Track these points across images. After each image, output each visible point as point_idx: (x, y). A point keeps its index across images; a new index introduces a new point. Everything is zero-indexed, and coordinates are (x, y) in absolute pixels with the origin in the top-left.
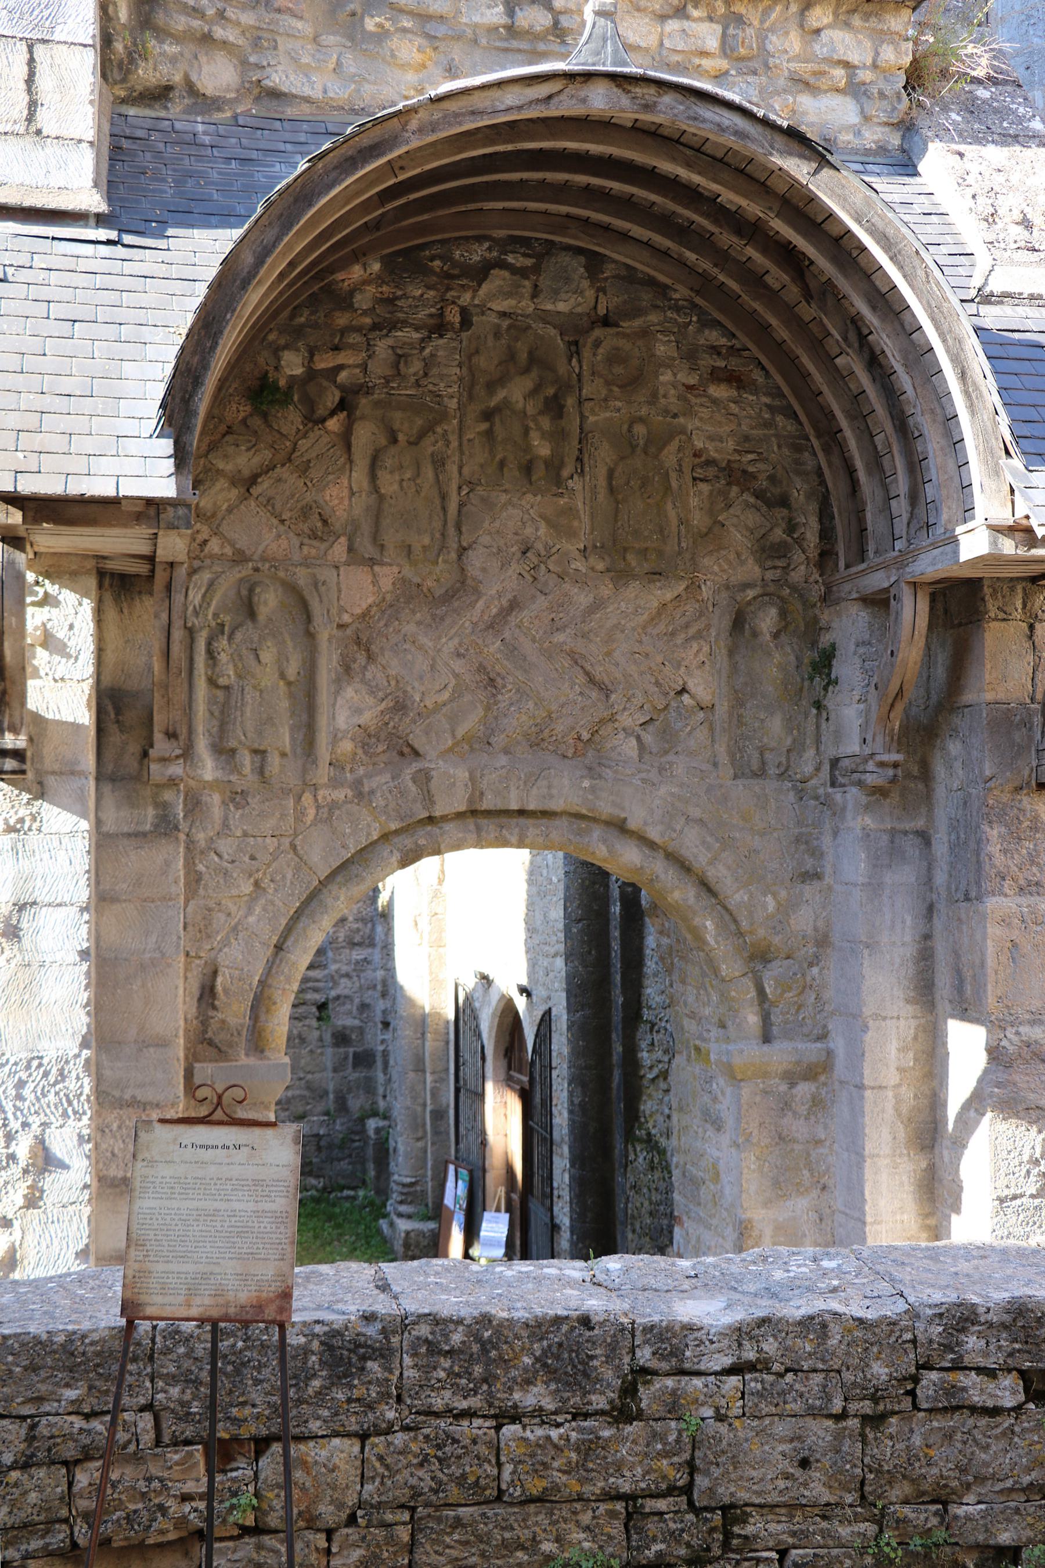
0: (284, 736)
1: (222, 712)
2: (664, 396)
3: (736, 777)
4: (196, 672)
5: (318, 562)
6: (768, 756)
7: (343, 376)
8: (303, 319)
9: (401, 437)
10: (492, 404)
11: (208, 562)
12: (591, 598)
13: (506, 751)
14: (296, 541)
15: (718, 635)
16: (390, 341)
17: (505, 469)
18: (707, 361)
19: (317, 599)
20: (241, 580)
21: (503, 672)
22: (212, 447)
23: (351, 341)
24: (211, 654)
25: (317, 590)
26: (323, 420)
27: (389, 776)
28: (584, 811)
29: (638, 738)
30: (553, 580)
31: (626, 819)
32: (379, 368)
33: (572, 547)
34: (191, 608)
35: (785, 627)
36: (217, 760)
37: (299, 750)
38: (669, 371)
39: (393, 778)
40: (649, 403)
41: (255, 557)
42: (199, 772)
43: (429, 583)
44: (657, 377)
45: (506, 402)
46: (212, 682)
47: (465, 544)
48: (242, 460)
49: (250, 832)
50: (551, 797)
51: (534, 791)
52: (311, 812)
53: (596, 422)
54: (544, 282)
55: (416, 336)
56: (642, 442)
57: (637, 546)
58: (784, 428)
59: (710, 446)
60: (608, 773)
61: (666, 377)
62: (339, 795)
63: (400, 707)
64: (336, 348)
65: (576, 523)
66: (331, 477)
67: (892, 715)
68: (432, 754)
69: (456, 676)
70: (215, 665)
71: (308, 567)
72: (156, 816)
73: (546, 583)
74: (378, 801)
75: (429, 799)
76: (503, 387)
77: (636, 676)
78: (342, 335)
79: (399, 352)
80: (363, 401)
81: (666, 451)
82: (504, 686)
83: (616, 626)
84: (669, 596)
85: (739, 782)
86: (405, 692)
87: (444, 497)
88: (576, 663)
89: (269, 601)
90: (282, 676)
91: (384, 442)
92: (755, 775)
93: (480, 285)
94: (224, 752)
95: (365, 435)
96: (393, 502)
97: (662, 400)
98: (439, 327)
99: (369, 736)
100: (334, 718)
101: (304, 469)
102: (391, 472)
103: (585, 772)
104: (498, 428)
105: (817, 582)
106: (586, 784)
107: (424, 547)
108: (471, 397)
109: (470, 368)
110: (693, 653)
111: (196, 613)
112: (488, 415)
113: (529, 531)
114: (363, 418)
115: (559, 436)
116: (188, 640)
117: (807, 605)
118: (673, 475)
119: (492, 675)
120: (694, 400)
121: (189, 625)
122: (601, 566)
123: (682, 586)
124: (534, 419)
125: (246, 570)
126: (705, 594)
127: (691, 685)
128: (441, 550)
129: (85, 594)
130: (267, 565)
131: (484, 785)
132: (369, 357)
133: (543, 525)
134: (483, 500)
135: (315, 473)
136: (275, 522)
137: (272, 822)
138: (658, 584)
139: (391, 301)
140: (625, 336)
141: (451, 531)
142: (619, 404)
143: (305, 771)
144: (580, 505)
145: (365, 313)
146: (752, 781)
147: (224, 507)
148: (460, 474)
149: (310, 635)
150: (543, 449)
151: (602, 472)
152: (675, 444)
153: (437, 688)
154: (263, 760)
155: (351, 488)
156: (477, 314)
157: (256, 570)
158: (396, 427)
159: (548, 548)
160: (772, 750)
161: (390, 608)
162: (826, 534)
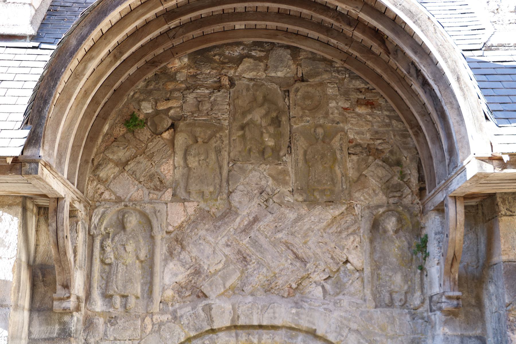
0: (138, 288)
1: (107, 277)
2: (332, 114)
3: (376, 307)
4: (94, 257)
5: (157, 201)
6: (395, 296)
7: (172, 112)
8: (152, 87)
9: (199, 140)
10: (245, 122)
11: (103, 203)
12: (296, 215)
13: (252, 294)
14: (146, 192)
15: (364, 232)
16: (194, 95)
17: (251, 153)
18: (355, 96)
19: (156, 219)
20: (119, 211)
21: (250, 254)
22: (107, 148)
23: (175, 95)
24: (102, 248)
25: (156, 215)
27: (190, 308)
28: (293, 326)
29: (323, 287)
30: (276, 206)
31: (315, 330)
32: (188, 108)
33: (285, 190)
34: (93, 225)
35: (402, 227)
36: (104, 301)
37: (145, 295)
38: (334, 102)
39: (192, 309)
40: (324, 117)
41: (126, 200)
42: (93, 307)
43: (213, 210)
44: (328, 105)
45: (252, 121)
46: (103, 262)
47: (231, 190)
48: (122, 154)
49: (118, 338)
50: (275, 318)
51: (266, 315)
52: (150, 327)
53: (297, 128)
54: (271, 62)
55: (207, 91)
56: (321, 137)
57: (320, 188)
58: (397, 126)
59: (357, 137)
60: (306, 305)
61: (333, 104)
62: (165, 318)
63: (197, 272)
64: (168, 99)
65: (287, 178)
66: (164, 160)
67: (453, 270)
68: (212, 295)
69: (226, 256)
70: (104, 253)
71: (151, 203)
72: (60, 329)
73: (273, 208)
74: (184, 321)
75: (211, 320)
76: (250, 113)
77: (320, 254)
78: (171, 93)
79: (199, 99)
80: (181, 124)
81: (334, 140)
82: (251, 261)
83: (309, 229)
84: (337, 213)
85: (378, 310)
86: (200, 265)
87: (221, 167)
88: (289, 248)
89: (133, 221)
90: (138, 258)
91: (191, 142)
92: (388, 306)
93: (238, 67)
94: (107, 297)
95: (181, 139)
97: (331, 116)
98: (219, 87)
99: (182, 287)
100: (163, 278)
101: (150, 157)
102: (194, 157)
103: (293, 305)
104: (248, 135)
105: (418, 204)
106: (294, 311)
107: (211, 192)
108: (234, 120)
109: (234, 106)
110: (350, 242)
111: (95, 228)
112: (243, 128)
113: (263, 183)
114: (181, 131)
115: (277, 136)
116: (91, 241)
117: (413, 215)
118: (338, 152)
119: (245, 255)
120: (347, 115)
121: (92, 233)
122: (300, 199)
123: (343, 208)
124: (266, 128)
125: (121, 206)
126: (356, 211)
127: (350, 259)
128: (219, 194)
129: (16, 215)
130: (131, 203)
131: (239, 312)
132: (184, 103)
133: (270, 179)
134: (240, 168)
135: (156, 159)
136: (137, 183)
137: (129, 333)
138: (331, 207)
139: (194, 76)
140: (311, 86)
141: (225, 184)
142: (308, 119)
143: (147, 306)
144: (290, 169)
145: (182, 82)
146: (386, 309)
147: (112, 176)
148: (229, 156)
149: (152, 237)
150: (270, 143)
151: (301, 152)
152: (338, 136)
153: (216, 262)
154: (127, 300)
155: (174, 165)
156: (237, 80)
157: (126, 206)
158: (198, 134)
159: (273, 190)
160: (396, 292)
161: (193, 223)
162: (421, 179)
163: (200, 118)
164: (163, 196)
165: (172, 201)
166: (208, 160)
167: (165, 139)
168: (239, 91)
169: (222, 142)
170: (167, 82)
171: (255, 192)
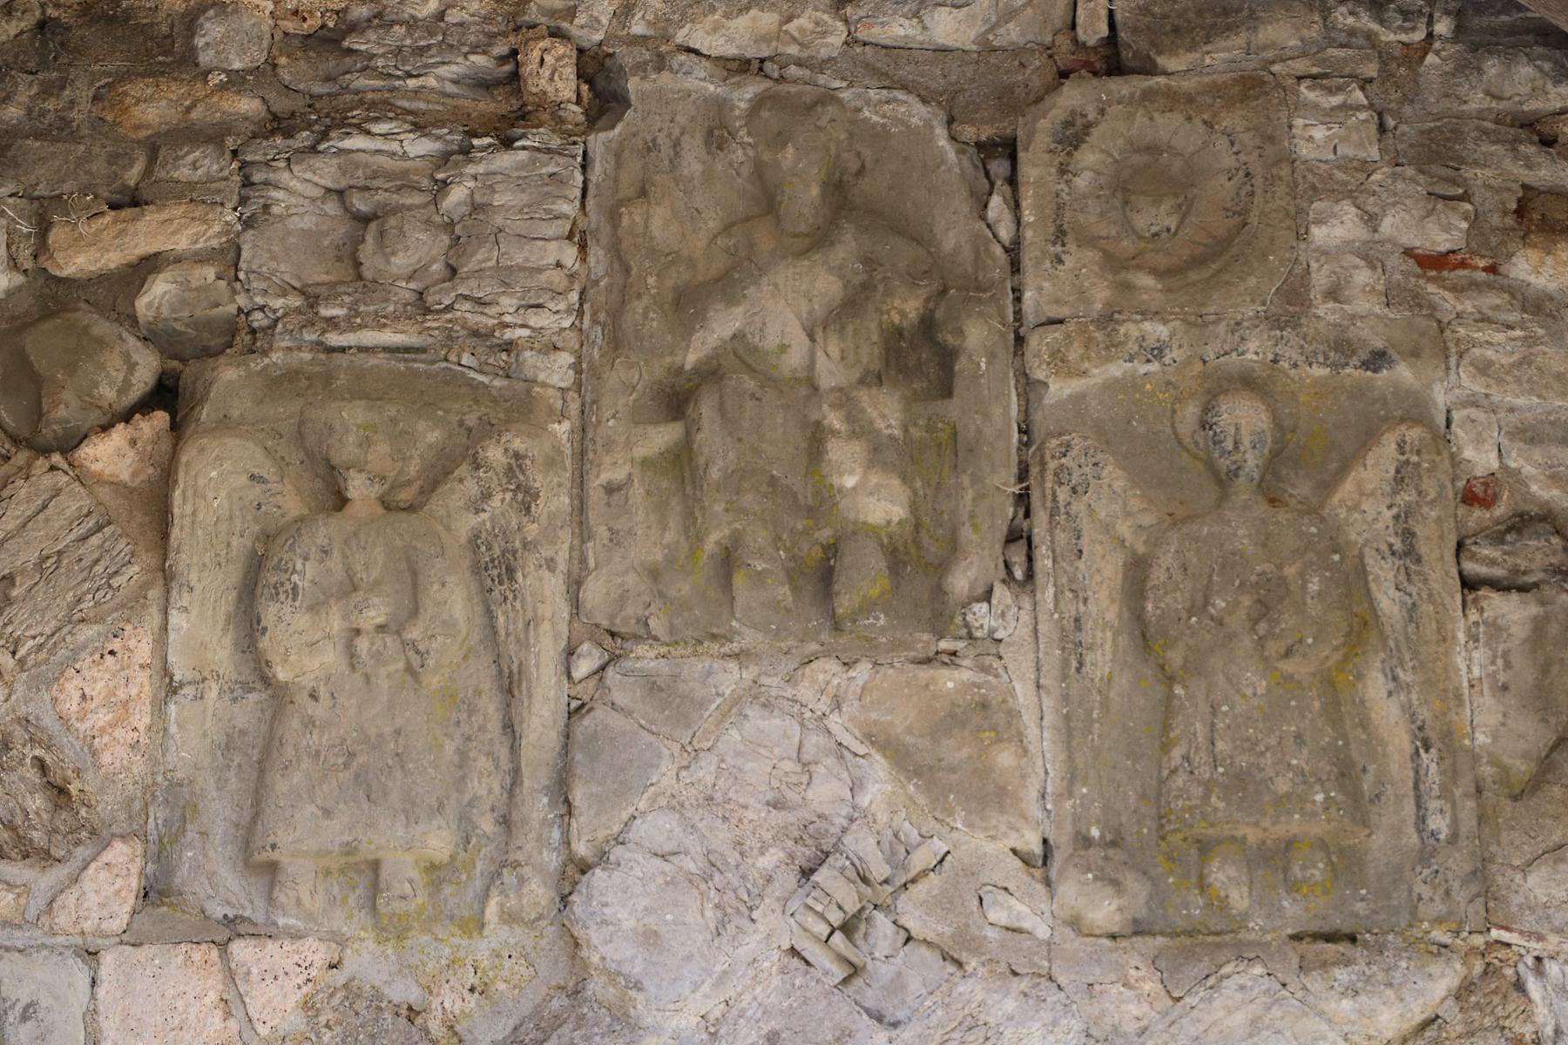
2: (1333, 294)
5: (19, 938)
7: (158, 294)
9: (358, 487)
10: (691, 359)
16: (324, 171)
17: (739, 580)
18: (1502, 170)
23: (183, 173)
26: (69, 443)
30: (921, 968)
32: (281, 260)
33: (991, 845)
38: (1349, 210)
40: (1276, 322)
43: (450, 1000)
44: (1302, 235)
45: (744, 352)
47: (581, 849)
53: (1078, 399)
55: (420, 147)
56: (1252, 461)
57: (1252, 835)
59: (1526, 463)
61: (1337, 228)
64: (131, 201)
65: (1005, 758)
66: (87, 633)
73: (897, 986)
76: (731, 300)
78: (152, 160)
79: (360, 204)
80: (228, 373)
81: (1348, 488)
87: (510, 685)
91: (293, 505)
95: (223, 482)
96: (319, 710)
97: (1325, 310)
98: (506, 111)
102: (314, 608)
104: (718, 450)
107: (432, 868)
108: (616, 343)
109: (616, 251)
112: (675, 401)
113: (826, 792)
114: (226, 424)
115: (931, 458)
120: (1449, 303)
122: (1105, 911)
123: (1441, 981)
124: (844, 399)
126: (1541, 1013)
128: (494, 876)
133: (878, 768)
134: (654, 687)
138: (1342, 975)
140: (1175, 100)
141: (537, 806)
142: (1157, 330)
144: (1023, 694)
145: (237, 81)
148: (576, 604)
150: (879, 502)
151: (1103, 573)
152: (1383, 457)
155: (166, 672)
156: (640, 68)
158: (346, 449)
159: (896, 852)
163: (369, 337)
164: (70, 898)
165: (132, 938)
166: (413, 634)
167: (99, 480)
168: (651, 147)
169: (526, 499)
170: (122, 77)
171: (768, 861)
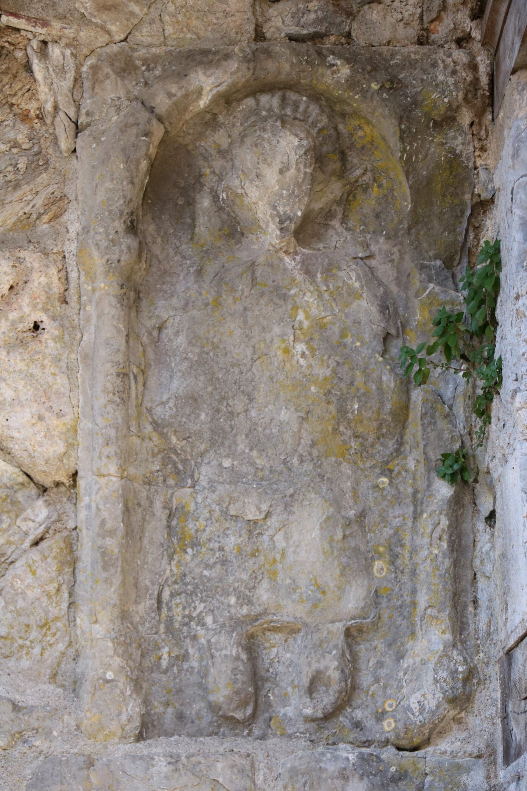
15: (86, 230)
35: (347, 201)
85: (158, 748)
92: (226, 723)
117: (417, 121)
126: (43, 89)
146: (211, 744)
160: (291, 630)
